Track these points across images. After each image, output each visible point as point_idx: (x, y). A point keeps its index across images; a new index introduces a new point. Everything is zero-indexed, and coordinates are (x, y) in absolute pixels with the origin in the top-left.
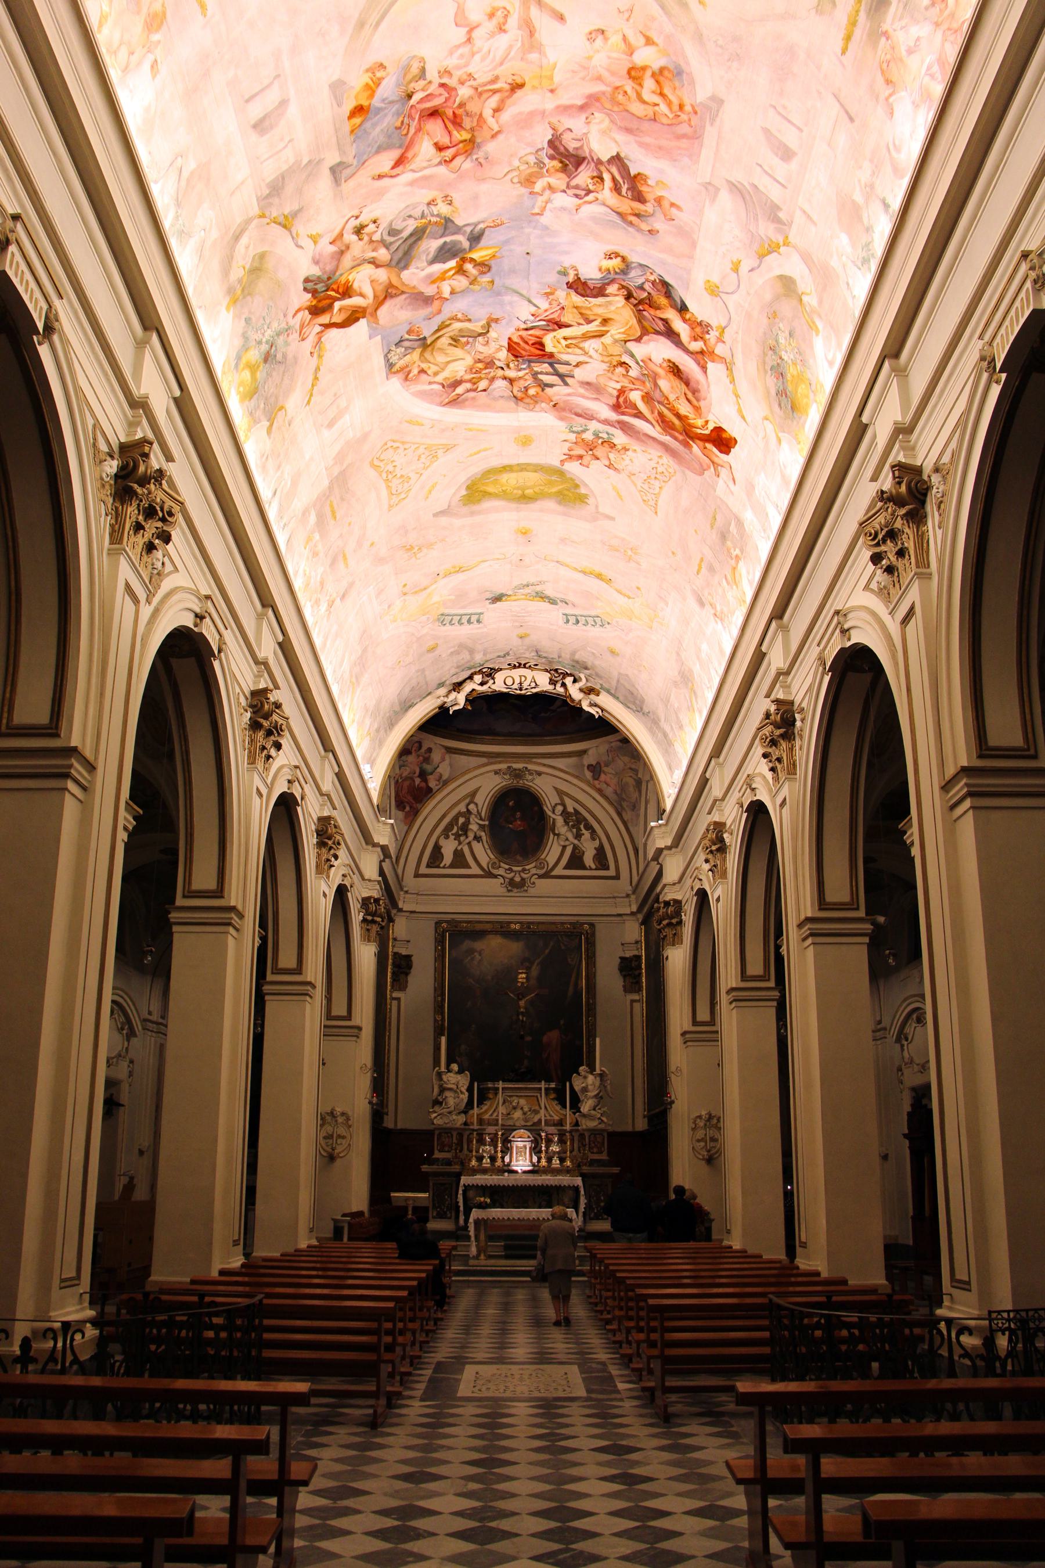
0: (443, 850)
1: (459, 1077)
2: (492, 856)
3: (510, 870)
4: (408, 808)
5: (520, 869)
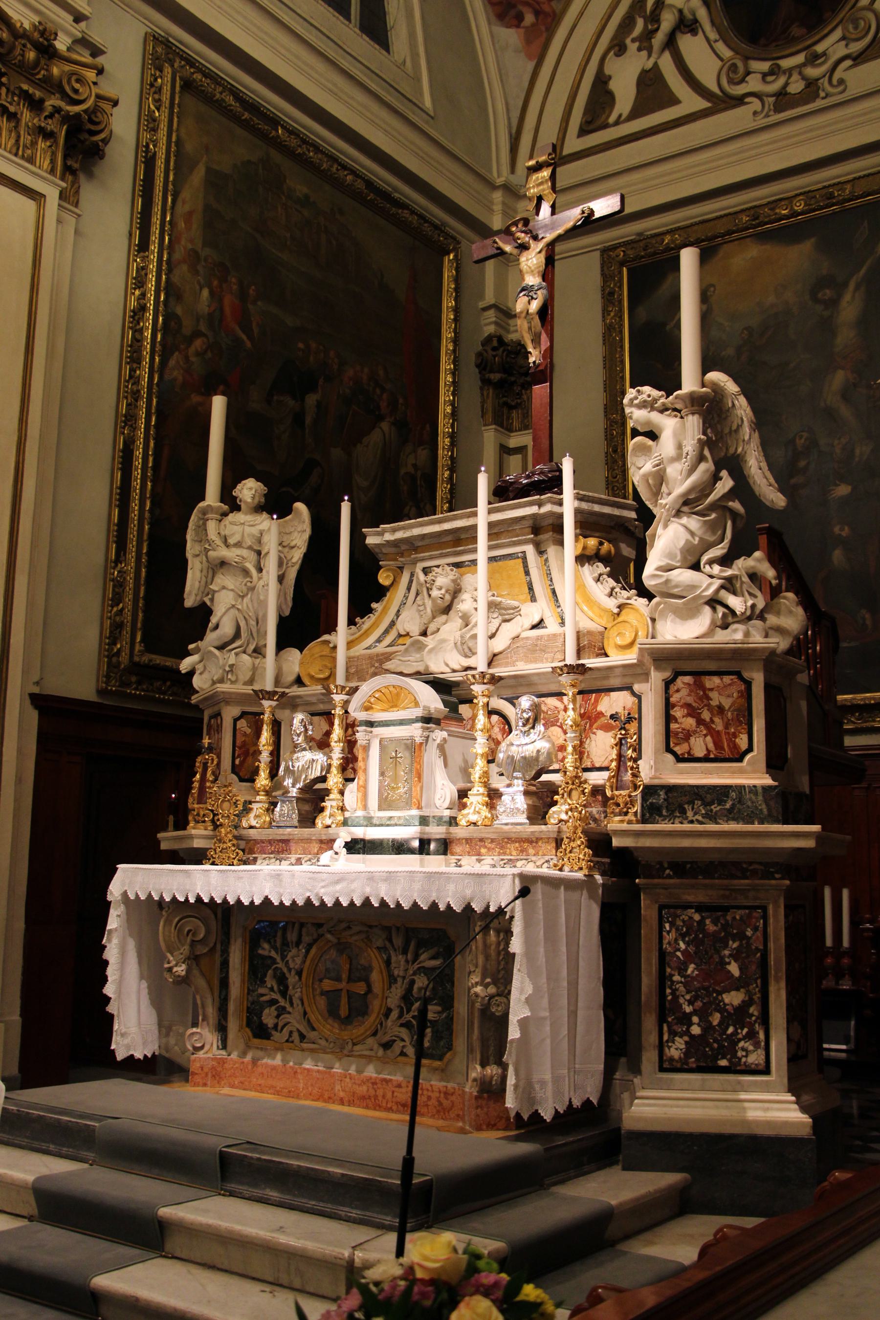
0: (613, 85)
1: (266, 523)
2: (727, 53)
3: (775, 71)
4: (529, 19)
5: (800, 58)
